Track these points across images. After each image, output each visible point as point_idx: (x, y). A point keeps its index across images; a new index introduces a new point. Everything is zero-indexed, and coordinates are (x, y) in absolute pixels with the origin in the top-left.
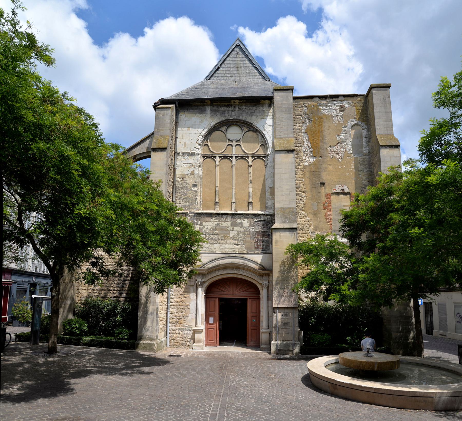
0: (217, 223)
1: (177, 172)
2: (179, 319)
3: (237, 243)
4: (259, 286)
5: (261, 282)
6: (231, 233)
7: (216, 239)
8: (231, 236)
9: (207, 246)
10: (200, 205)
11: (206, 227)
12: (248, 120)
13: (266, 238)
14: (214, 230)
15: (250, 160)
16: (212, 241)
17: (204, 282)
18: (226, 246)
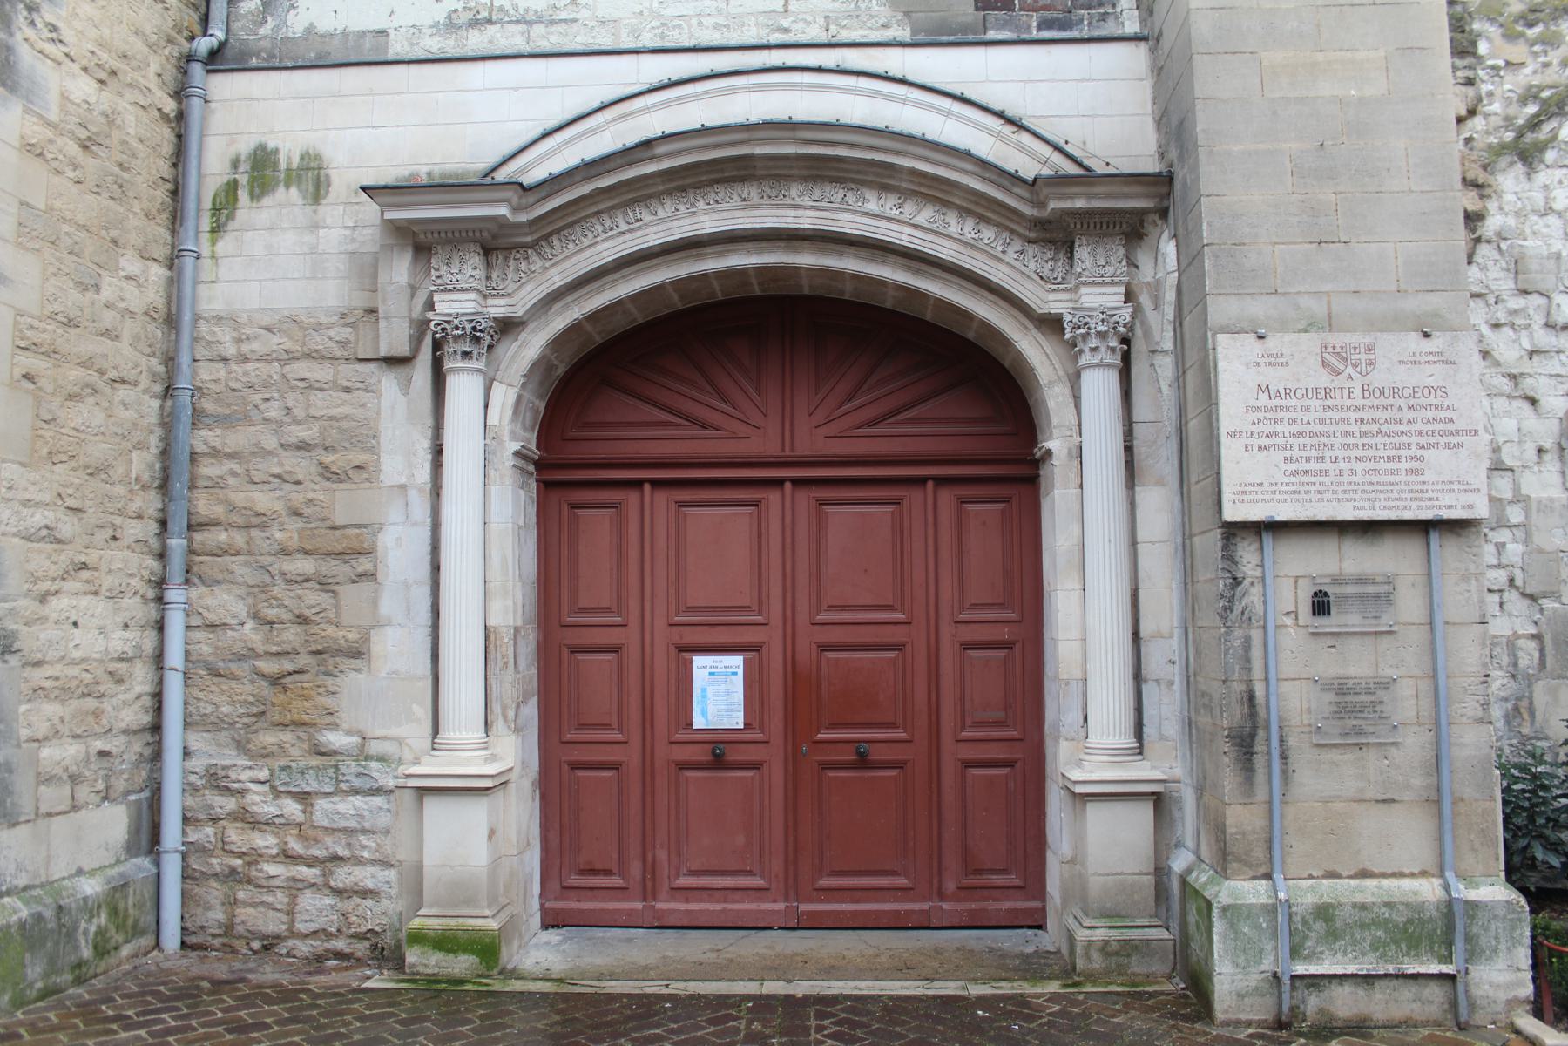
2: (276, 681)
4: (1033, 349)
5: (1057, 303)
17: (507, 327)
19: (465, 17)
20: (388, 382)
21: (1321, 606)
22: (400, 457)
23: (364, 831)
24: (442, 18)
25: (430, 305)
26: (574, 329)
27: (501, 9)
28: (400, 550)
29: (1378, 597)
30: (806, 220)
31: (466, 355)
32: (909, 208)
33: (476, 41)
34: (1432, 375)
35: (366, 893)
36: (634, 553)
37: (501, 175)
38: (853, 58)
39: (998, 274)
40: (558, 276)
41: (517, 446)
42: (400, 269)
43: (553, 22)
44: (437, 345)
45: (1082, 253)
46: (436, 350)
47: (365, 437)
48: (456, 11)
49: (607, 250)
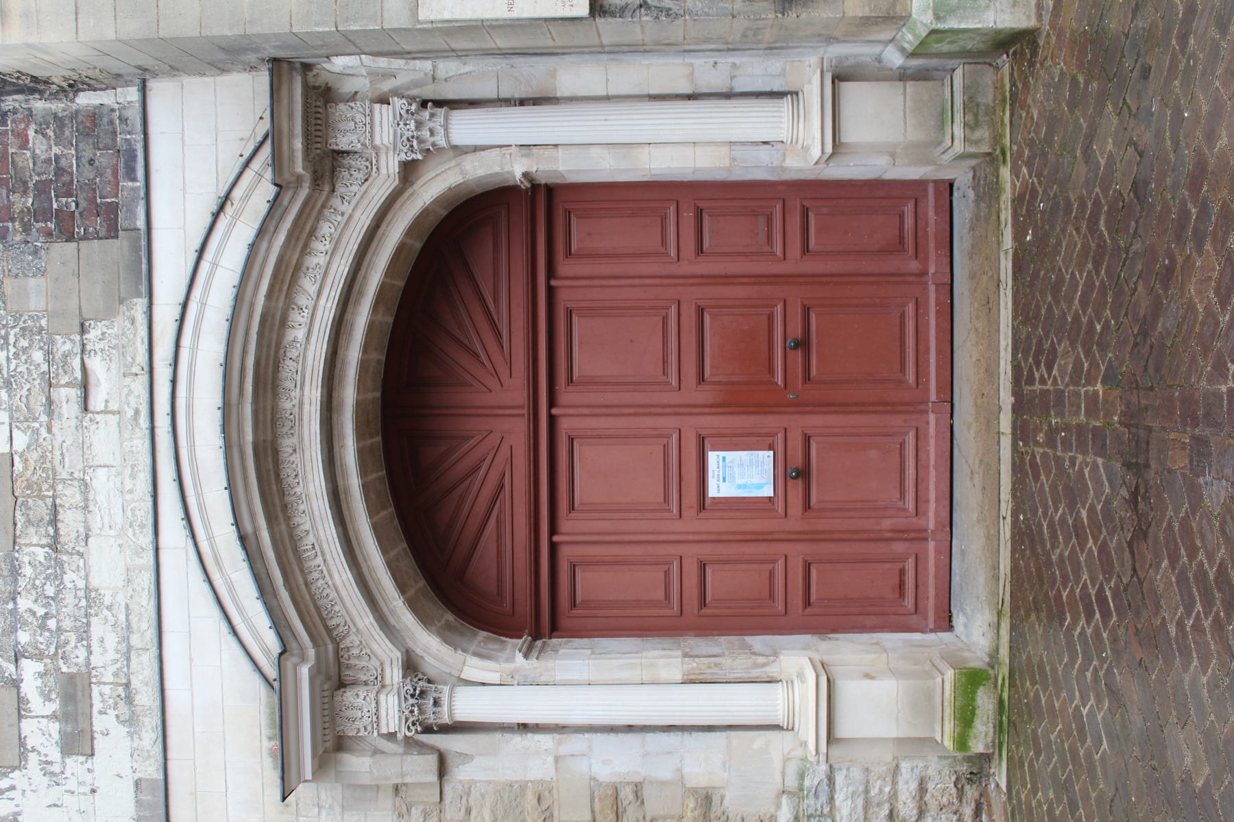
3: (74, 393)
5: (390, 166)
7: (56, 569)
8: (21, 441)
9: (112, 640)
13: (24, 144)
16: (69, 598)
17: (411, 666)
18: (101, 482)
19: (123, 709)
20: (461, 774)
22: (530, 761)
23: (867, 791)
24: (123, 730)
25: (391, 736)
26: (412, 605)
27: (116, 675)
28: (613, 762)
30: (313, 394)
31: (436, 703)
32: (302, 300)
33: (146, 698)
35: (922, 789)
36: (616, 550)
37: (272, 673)
39: (363, 220)
40: (365, 620)
41: (519, 657)
42: (358, 764)
43: (129, 627)
44: (428, 730)
45: (343, 143)
46: (432, 730)
47: (511, 796)
48: (117, 716)
49: (340, 575)
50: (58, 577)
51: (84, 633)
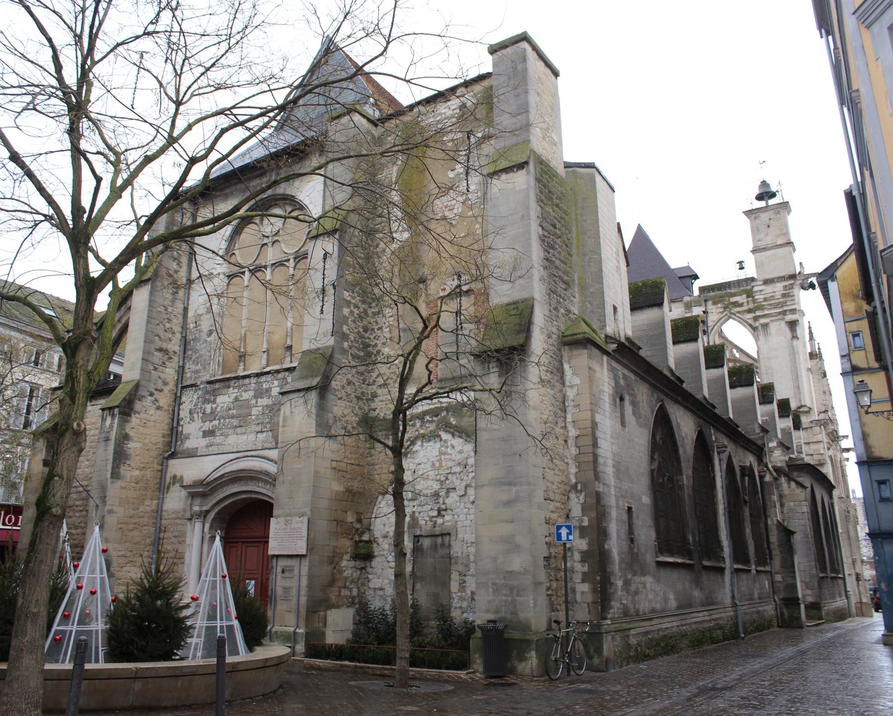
0: (235, 395)
1: (191, 314)
6: (255, 411)
10: (219, 365)
11: (221, 405)
12: (289, 192)
14: (230, 409)
15: (292, 263)
18: (245, 437)
21: (283, 572)
29: (291, 570)
34: (299, 525)
38: (260, 453)
40: (214, 502)
49: (221, 496)
50: (231, 428)
51: (221, 435)
